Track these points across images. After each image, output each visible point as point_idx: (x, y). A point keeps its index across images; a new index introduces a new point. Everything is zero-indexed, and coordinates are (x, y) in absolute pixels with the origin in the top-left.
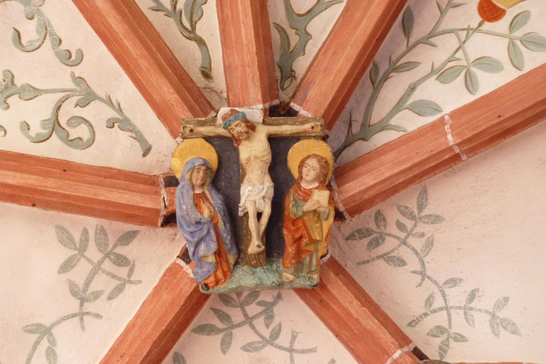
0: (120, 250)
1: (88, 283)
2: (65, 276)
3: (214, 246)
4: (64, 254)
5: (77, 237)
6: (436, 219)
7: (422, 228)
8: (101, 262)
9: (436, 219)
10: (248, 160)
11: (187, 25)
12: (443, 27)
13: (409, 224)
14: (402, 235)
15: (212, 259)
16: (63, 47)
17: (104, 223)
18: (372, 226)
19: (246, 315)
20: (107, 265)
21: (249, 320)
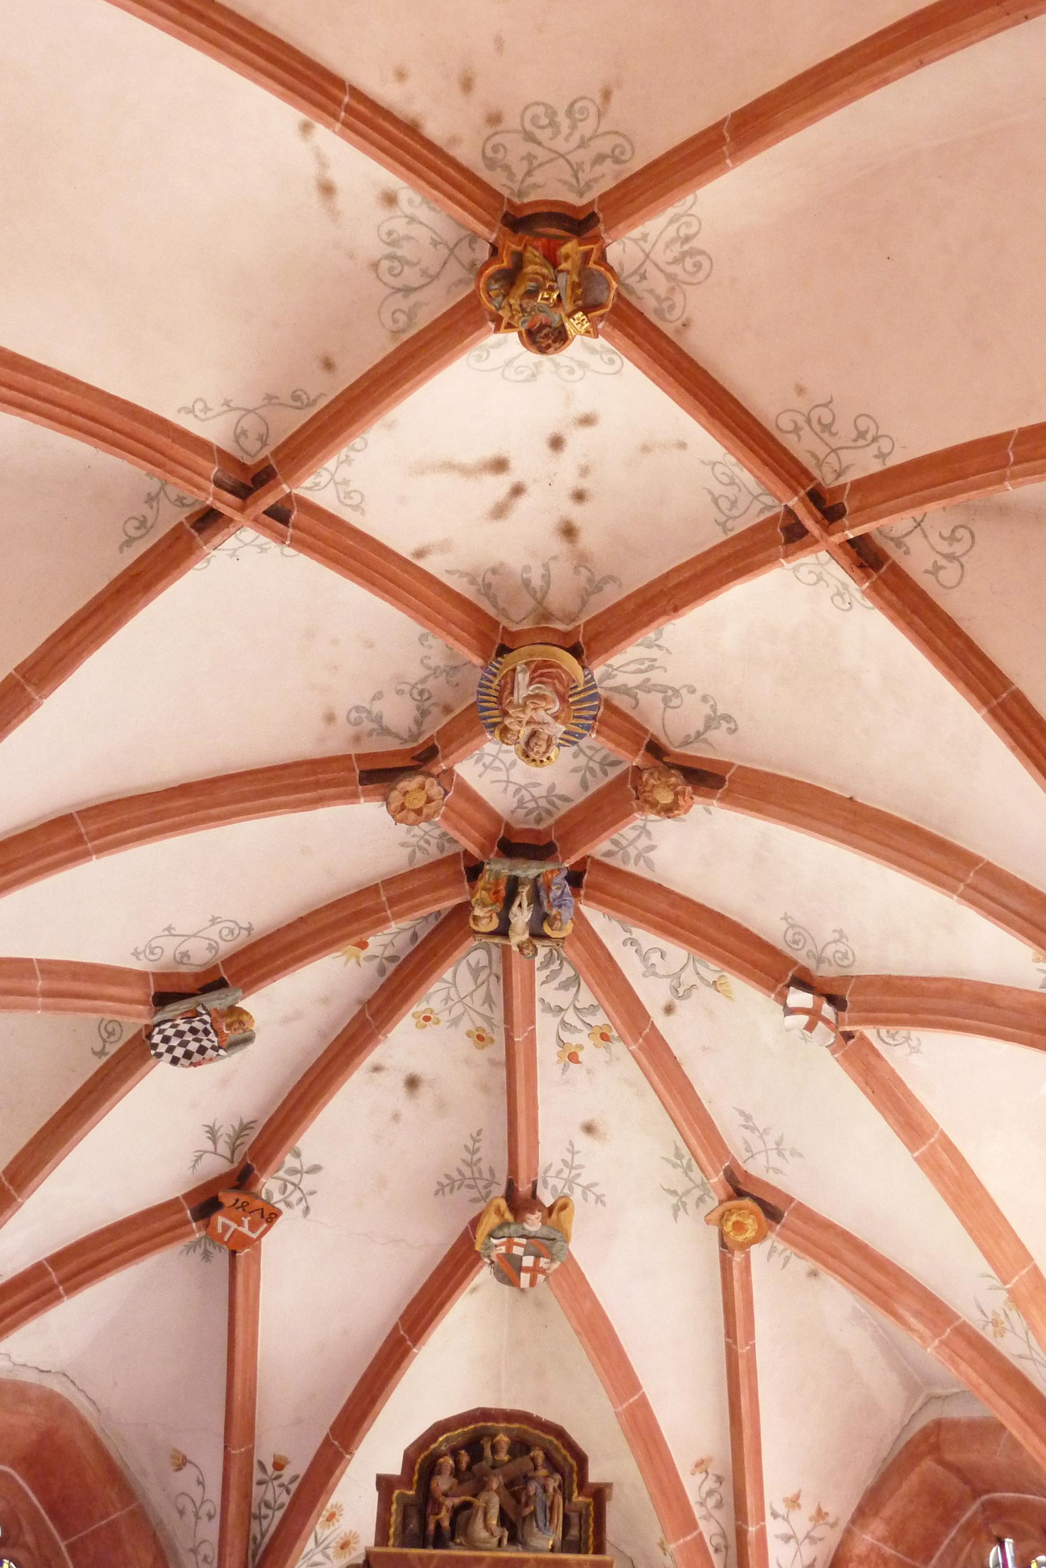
0: (616, 849)
1: (639, 836)
2: (653, 843)
3: (551, 895)
4: (651, 855)
5: (642, 862)
6: (403, 845)
7: (414, 840)
8: (629, 845)
9: (403, 845)
10: (523, 934)
11: (554, 951)
12: (392, 936)
13: (422, 843)
14: (427, 837)
15: (554, 888)
16: (635, 948)
17: (623, 867)
18: (446, 845)
19: (537, 802)
20: (624, 843)
21: (534, 799)
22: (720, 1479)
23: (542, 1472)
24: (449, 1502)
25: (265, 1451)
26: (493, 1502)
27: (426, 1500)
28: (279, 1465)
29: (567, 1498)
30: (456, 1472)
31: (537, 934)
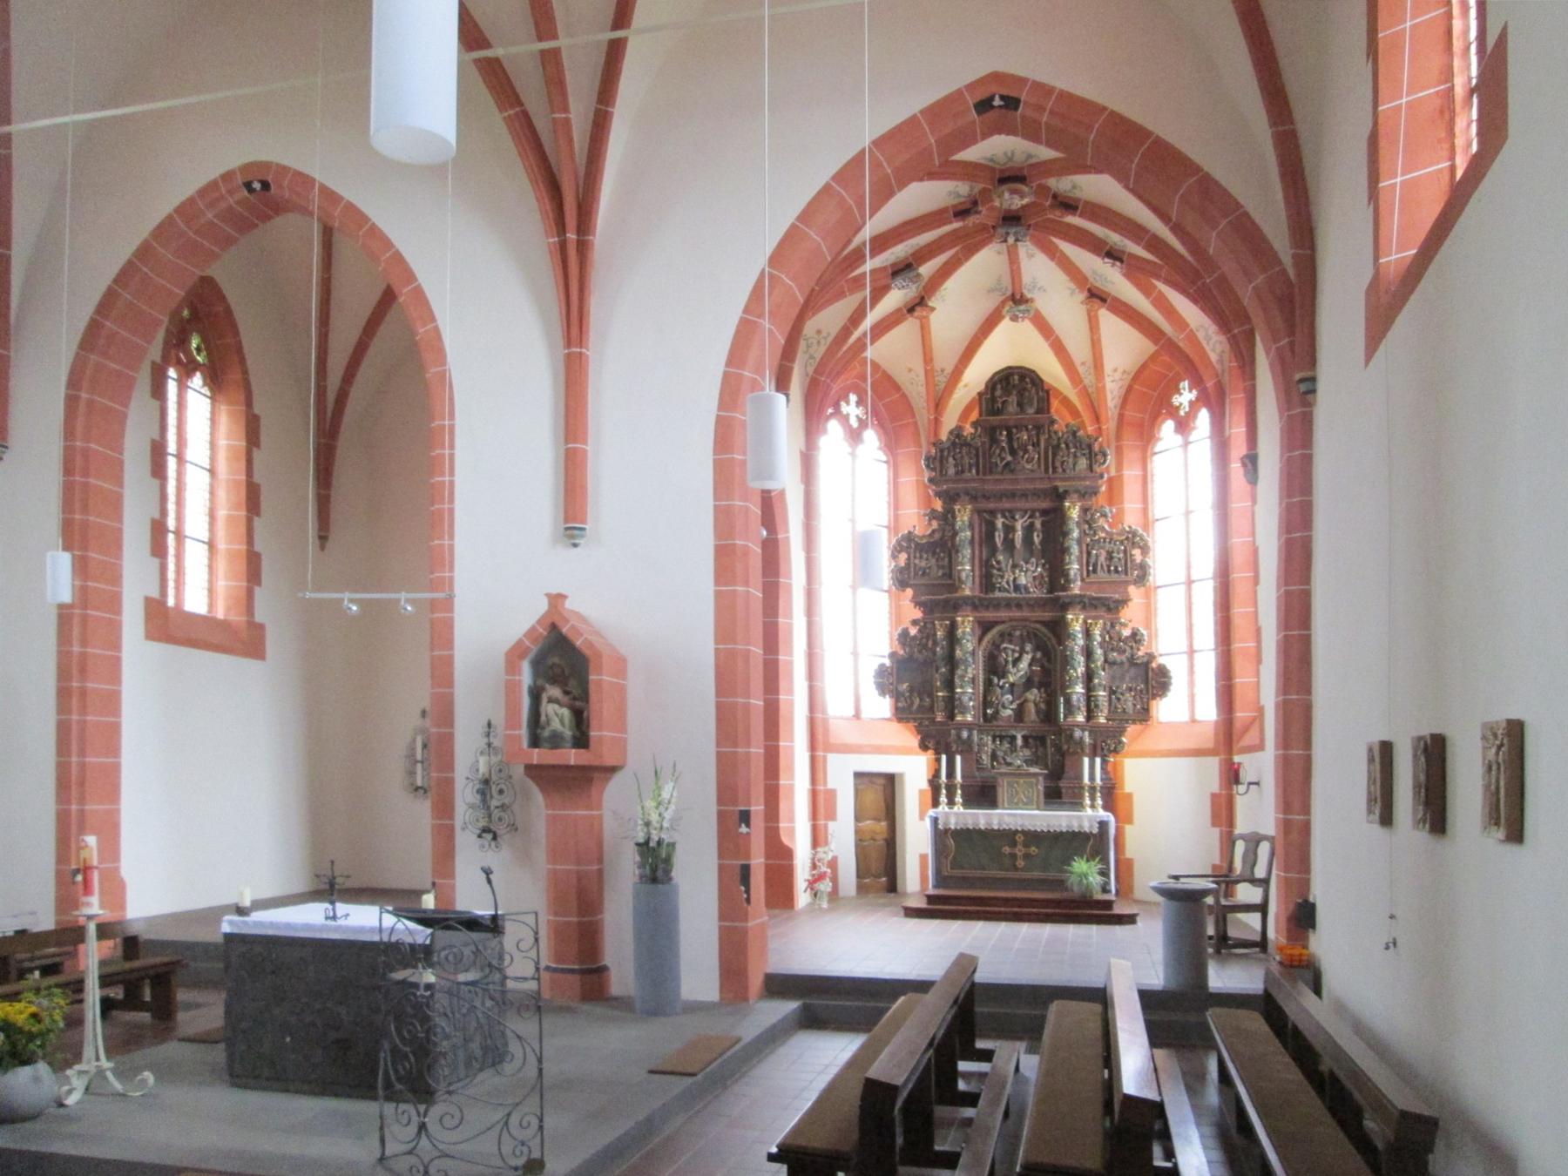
23: (1030, 386)
24: (1000, 400)
25: (938, 364)
26: (1013, 399)
27: (993, 400)
28: (943, 371)
29: (1038, 393)
30: (1002, 388)
31: (1017, 240)
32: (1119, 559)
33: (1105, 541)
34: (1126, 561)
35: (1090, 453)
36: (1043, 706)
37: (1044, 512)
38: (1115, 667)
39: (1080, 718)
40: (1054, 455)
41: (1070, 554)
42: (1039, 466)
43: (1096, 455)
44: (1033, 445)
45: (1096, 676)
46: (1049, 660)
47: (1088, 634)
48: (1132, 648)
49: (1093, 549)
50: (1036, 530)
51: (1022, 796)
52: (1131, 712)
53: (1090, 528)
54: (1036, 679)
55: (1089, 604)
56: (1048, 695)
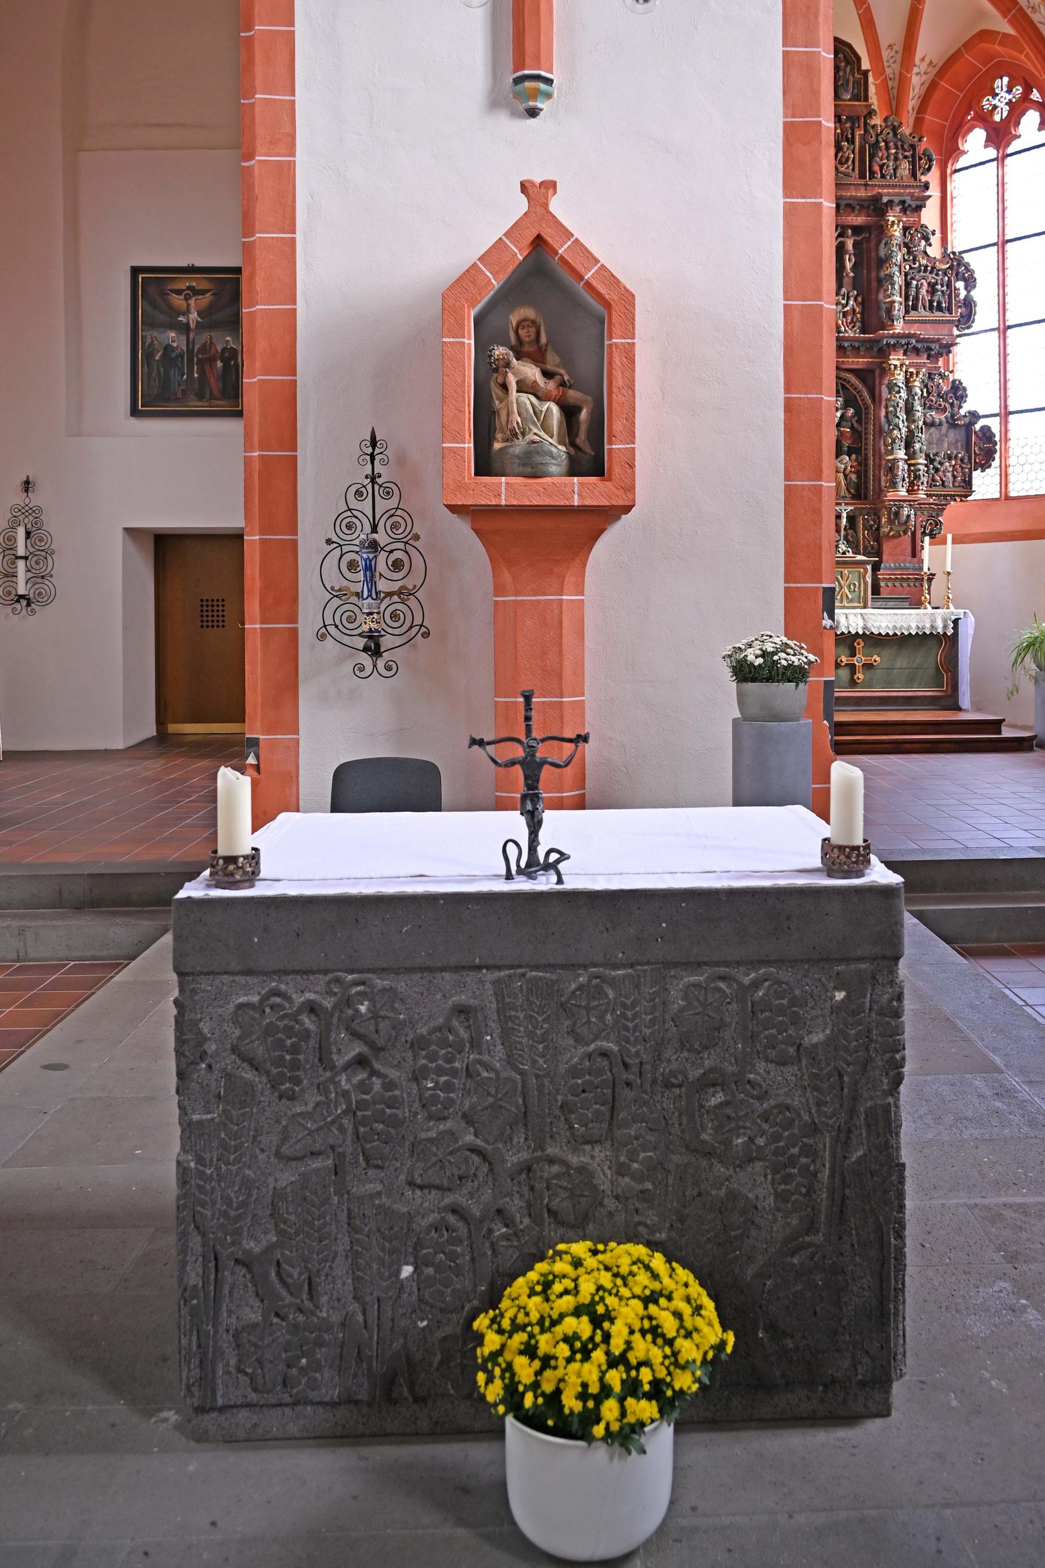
22: (897, 52)
32: (943, 292)
33: (925, 271)
34: (950, 296)
35: (913, 156)
36: (853, 477)
37: (857, 230)
38: (933, 429)
39: (903, 492)
40: (872, 157)
41: (893, 284)
42: (853, 170)
43: (920, 159)
44: (847, 140)
45: (916, 439)
46: (859, 421)
47: (909, 389)
48: (952, 405)
49: (913, 279)
50: (847, 252)
51: (847, 591)
52: (951, 485)
53: (909, 253)
54: (846, 444)
55: (914, 347)
56: (860, 464)
